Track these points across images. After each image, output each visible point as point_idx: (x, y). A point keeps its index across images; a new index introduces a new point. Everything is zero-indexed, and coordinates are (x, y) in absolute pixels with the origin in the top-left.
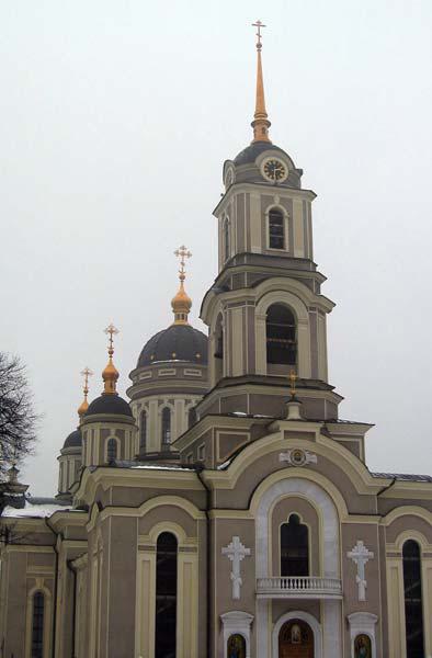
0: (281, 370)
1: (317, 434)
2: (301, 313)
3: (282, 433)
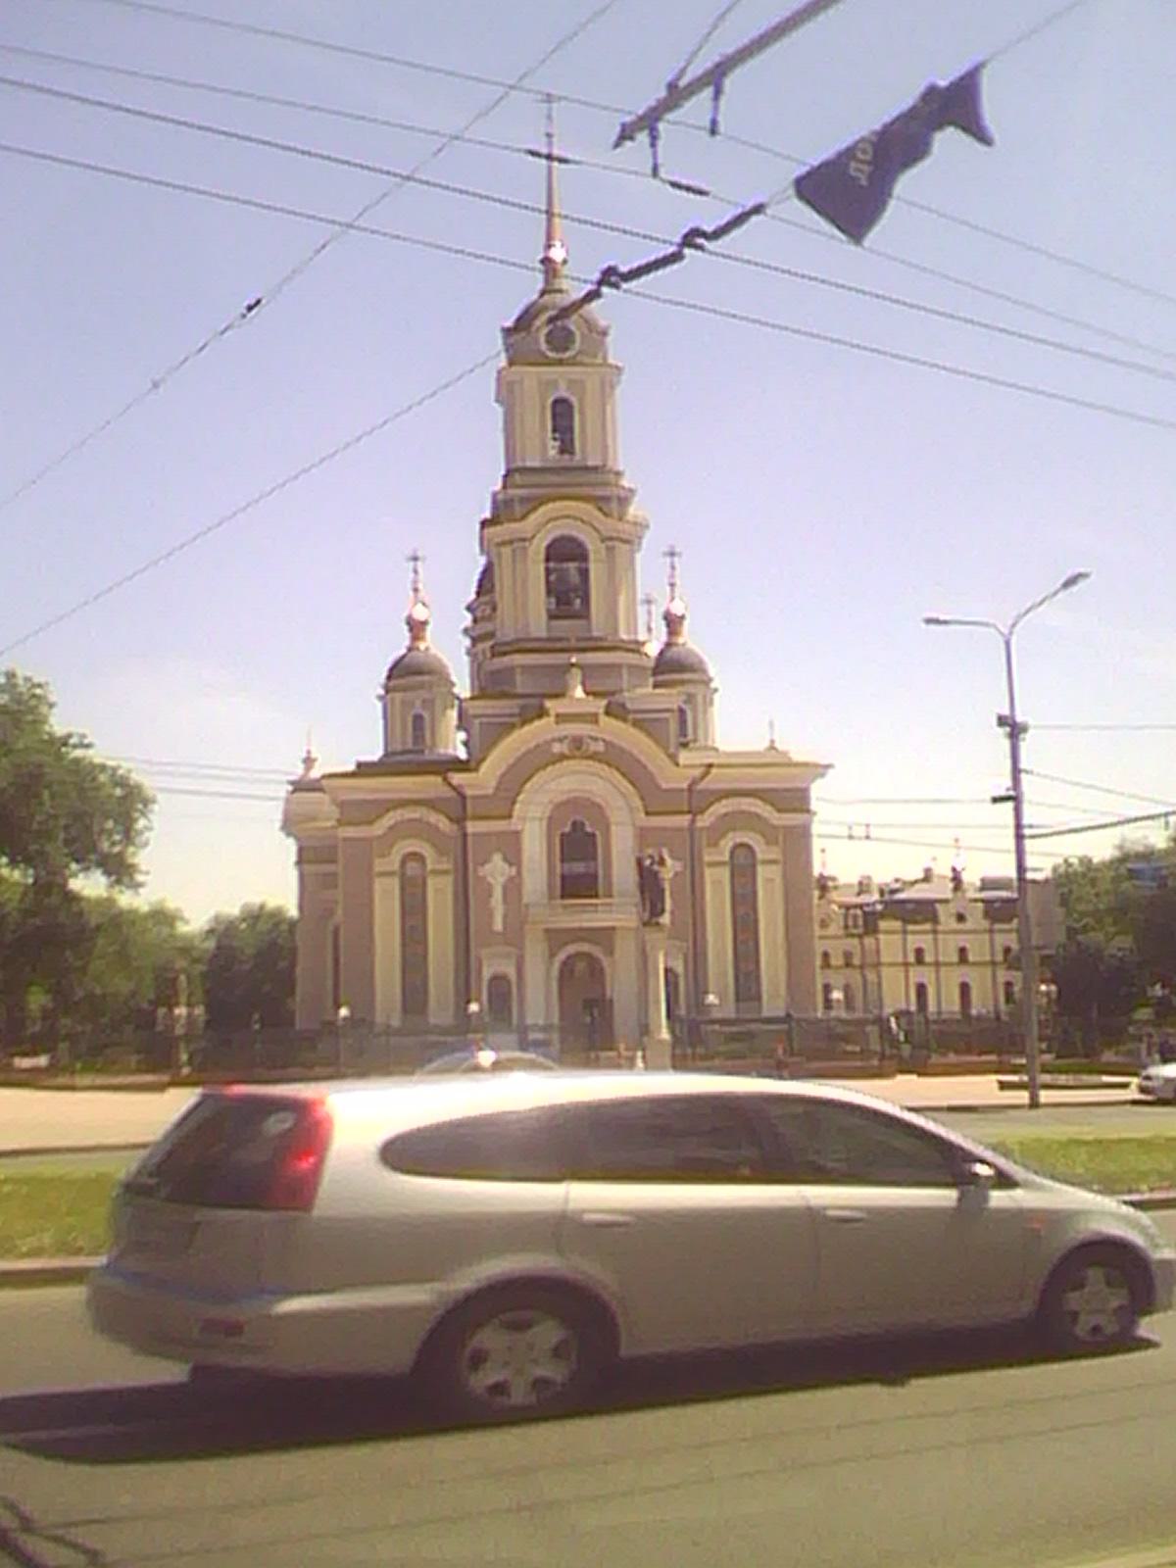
2: (593, 545)
3: (552, 719)
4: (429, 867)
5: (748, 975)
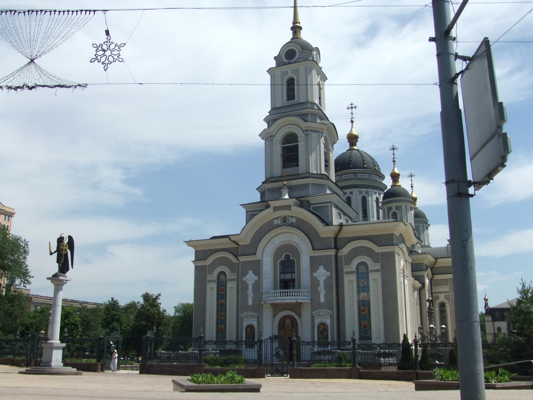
0: (290, 171)
1: (292, 206)
2: (301, 135)
4: (228, 278)
5: (365, 326)
